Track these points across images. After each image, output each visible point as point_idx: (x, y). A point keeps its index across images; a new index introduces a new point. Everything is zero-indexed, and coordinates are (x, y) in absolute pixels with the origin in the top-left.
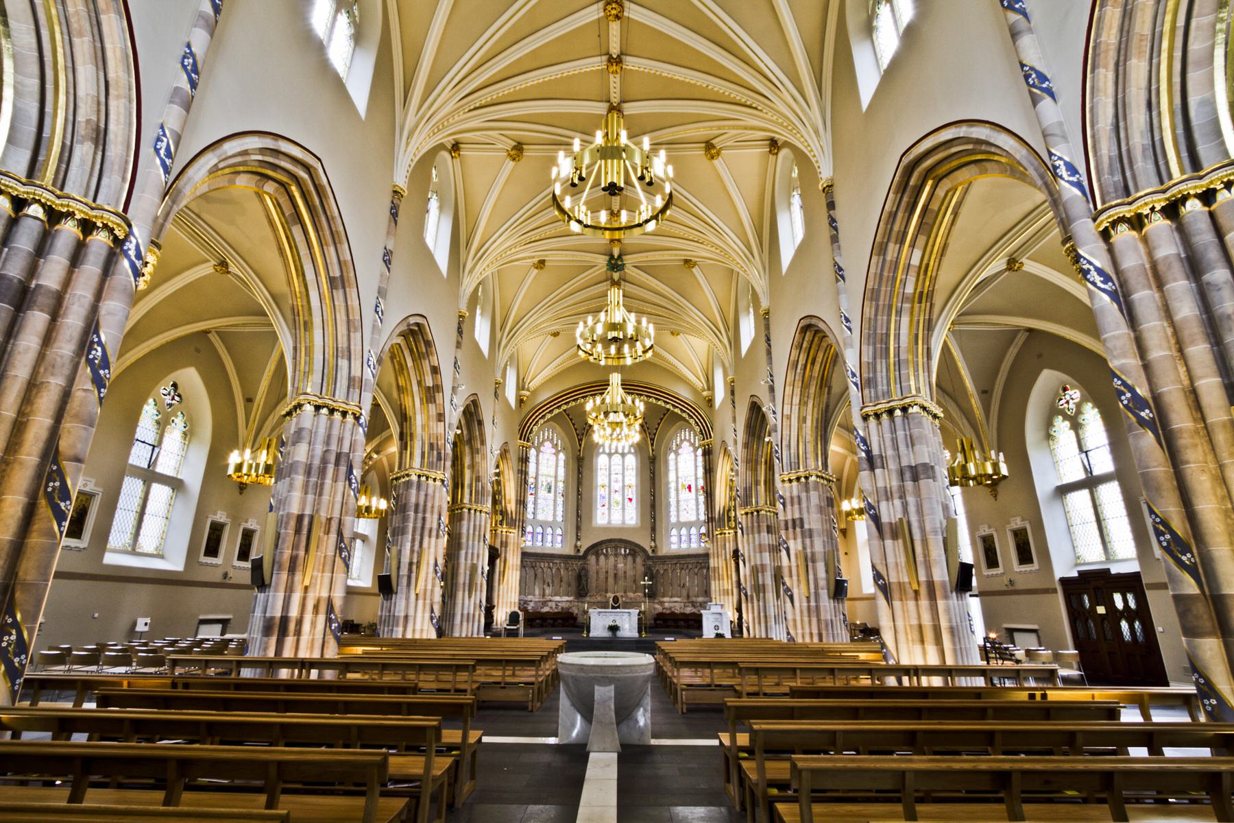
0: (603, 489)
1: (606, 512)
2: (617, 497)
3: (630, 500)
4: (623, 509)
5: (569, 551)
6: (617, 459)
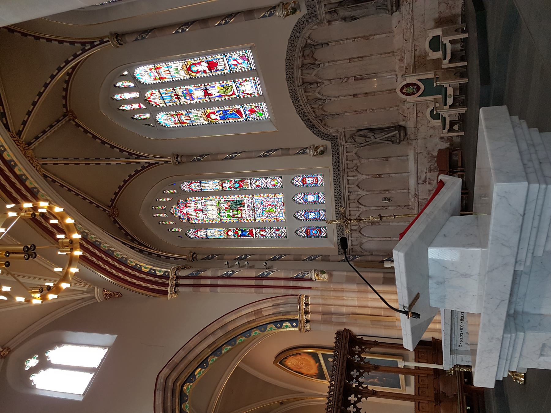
0: (213, 116)
1: (248, 106)
2: (215, 89)
3: (212, 65)
4: (233, 76)
5: (328, 159)
6: (155, 97)
